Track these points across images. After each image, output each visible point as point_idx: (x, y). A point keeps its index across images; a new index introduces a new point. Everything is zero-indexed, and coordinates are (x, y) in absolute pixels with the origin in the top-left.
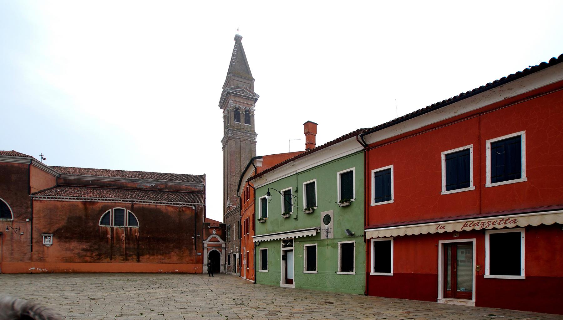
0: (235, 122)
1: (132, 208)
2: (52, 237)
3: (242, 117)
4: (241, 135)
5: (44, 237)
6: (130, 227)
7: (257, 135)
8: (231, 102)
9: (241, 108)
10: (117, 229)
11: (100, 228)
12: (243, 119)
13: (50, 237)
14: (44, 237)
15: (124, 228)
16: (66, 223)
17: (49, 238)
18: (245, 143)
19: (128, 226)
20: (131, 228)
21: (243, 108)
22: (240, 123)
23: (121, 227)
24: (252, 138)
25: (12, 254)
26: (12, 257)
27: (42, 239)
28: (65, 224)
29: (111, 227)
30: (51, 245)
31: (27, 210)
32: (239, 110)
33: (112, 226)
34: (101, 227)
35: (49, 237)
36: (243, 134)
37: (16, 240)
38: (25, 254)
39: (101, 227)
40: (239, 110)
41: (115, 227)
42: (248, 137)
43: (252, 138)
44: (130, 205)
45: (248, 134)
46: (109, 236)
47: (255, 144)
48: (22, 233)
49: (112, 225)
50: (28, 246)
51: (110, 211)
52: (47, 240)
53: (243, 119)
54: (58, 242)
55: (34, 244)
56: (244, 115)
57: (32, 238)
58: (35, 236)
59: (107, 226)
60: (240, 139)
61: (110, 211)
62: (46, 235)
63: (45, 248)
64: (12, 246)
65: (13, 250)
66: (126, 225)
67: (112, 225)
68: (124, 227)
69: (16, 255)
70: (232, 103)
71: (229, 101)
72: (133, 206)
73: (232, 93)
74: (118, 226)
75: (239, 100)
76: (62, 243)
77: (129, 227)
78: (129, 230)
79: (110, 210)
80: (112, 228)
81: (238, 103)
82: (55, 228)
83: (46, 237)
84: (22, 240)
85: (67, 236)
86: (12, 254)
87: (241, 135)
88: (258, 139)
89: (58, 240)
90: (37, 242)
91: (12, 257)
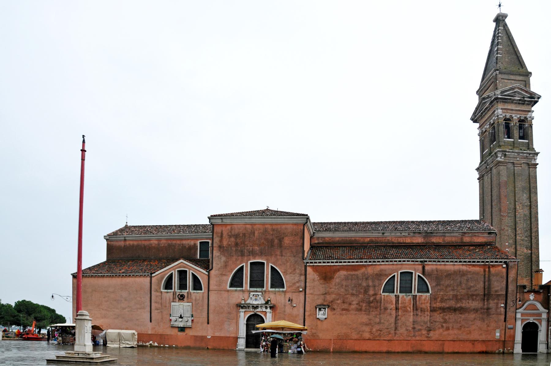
0: (505, 139)
2: (327, 309)
3: (515, 132)
4: (515, 158)
5: (318, 309)
7: (537, 154)
8: (500, 111)
9: (514, 118)
10: (403, 296)
11: (382, 296)
12: (516, 133)
13: (325, 309)
15: (411, 296)
17: (324, 310)
18: (521, 168)
19: (416, 293)
22: (512, 140)
23: (409, 295)
24: (530, 159)
27: (316, 311)
29: (396, 295)
30: (326, 318)
31: (300, 278)
32: (510, 121)
33: (397, 294)
35: (323, 309)
36: (518, 155)
39: (383, 295)
40: (510, 121)
41: (401, 295)
42: (524, 158)
43: (530, 159)
45: (525, 155)
47: (534, 168)
48: (295, 305)
53: (516, 133)
56: (518, 128)
59: (390, 294)
60: (513, 163)
61: (394, 276)
67: (397, 292)
68: (412, 295)
70: (500, 113)
71: (494, 111)
73: (501, 98)
74: (404, 294)
75: (510, 106)
77: (418, 294)
81: (509, 111)
83: (320, 310)
87: (515, 158)
88: (539, 160)
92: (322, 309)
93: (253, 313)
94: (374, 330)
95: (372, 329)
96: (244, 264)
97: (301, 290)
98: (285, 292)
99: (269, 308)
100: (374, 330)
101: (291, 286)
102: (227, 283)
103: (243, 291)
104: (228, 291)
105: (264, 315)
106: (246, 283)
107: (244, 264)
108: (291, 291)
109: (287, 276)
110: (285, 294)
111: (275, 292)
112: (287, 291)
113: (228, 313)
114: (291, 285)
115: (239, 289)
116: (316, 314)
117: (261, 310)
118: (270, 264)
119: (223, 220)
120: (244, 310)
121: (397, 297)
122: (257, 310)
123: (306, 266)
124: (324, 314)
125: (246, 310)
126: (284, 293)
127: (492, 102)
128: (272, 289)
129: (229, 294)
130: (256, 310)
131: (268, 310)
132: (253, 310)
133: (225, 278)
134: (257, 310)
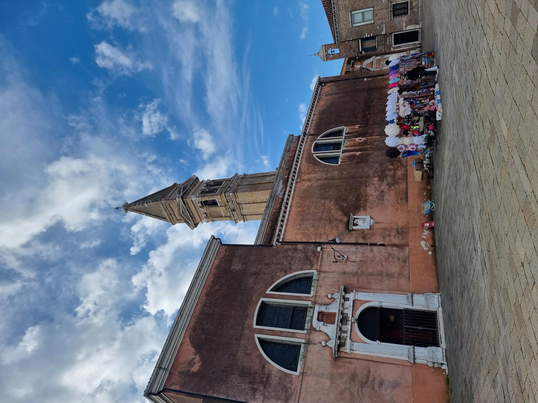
1: (316, 135)
5: (354, 227)
6: (344, 134)
7: (236, 175)
13: (355, 219)
14: (354, 227)
16: (331, 201)
19: (343, 137)
20: (346, 134)
21: (203, 188)
25: (390, 276)
26: (396, 275)
28: (332, 202)
30: (371, 218)
34: (341, 162)
37: (359, 269)
38: (389, 255)
44: (310, 137)
46: (358, 153)
49: (340, 152)
50: (372, 250)
51: (316, 156)
52: (360, 222)
54: (365, 209)
55: (369, 242)
57: (356, 244)
58: (353, 240)
62: (351, 221)
63: (377, 226)
64: (372, 274)
65: (381, 274)
66: (342, 138)
69: (394, 268)
72: (311, 135)
74: (342, 146)
76: (368, 205)
77: (344, 136)
78: (346, 135)
79: (314, 155)
80: (343, 152)
82: (338, 214)
84: (358, 259)
85: (354, 199)
86: (390, 276)
89: (362, 209)
90: (364, 238)
91: (396, 275)
92: (355, 222)
93: (356, 326)
94: (391, 167)
95: (390, 170)
96: (256, 336)
97: (319, 249)
98: (320, 272)
99: (347, 296)
100: (391, 167)
101: (311, 263)
102: (286, 374)
103: (308, 343)
104: (303, 373)
105: (361, 304)
106: (293, 335)
107: (256, 336)
108: (319, 262)
109: (294, 268)
110: (325, 272)
111: (318, 287)
112: (319, 268)
113: (353, 380)
114: (309, 263)
115: (302, 350)
116: (363, 231)
117: (351, 308)
118: (268, 292)
119: (163, 366)
120: (348, 342)
121: (343, 152)
122: (350, 316)
123: (284, 243)
124: (364, 220)
125: (349, 338)
126: (322, 275)
127: (184, 203)
128: (312, 292)
129: (309, 372)
130: (350, 319)
131: (351, 296)
132: (350, 323)
133: (274, 380)
134: (350, 316)
